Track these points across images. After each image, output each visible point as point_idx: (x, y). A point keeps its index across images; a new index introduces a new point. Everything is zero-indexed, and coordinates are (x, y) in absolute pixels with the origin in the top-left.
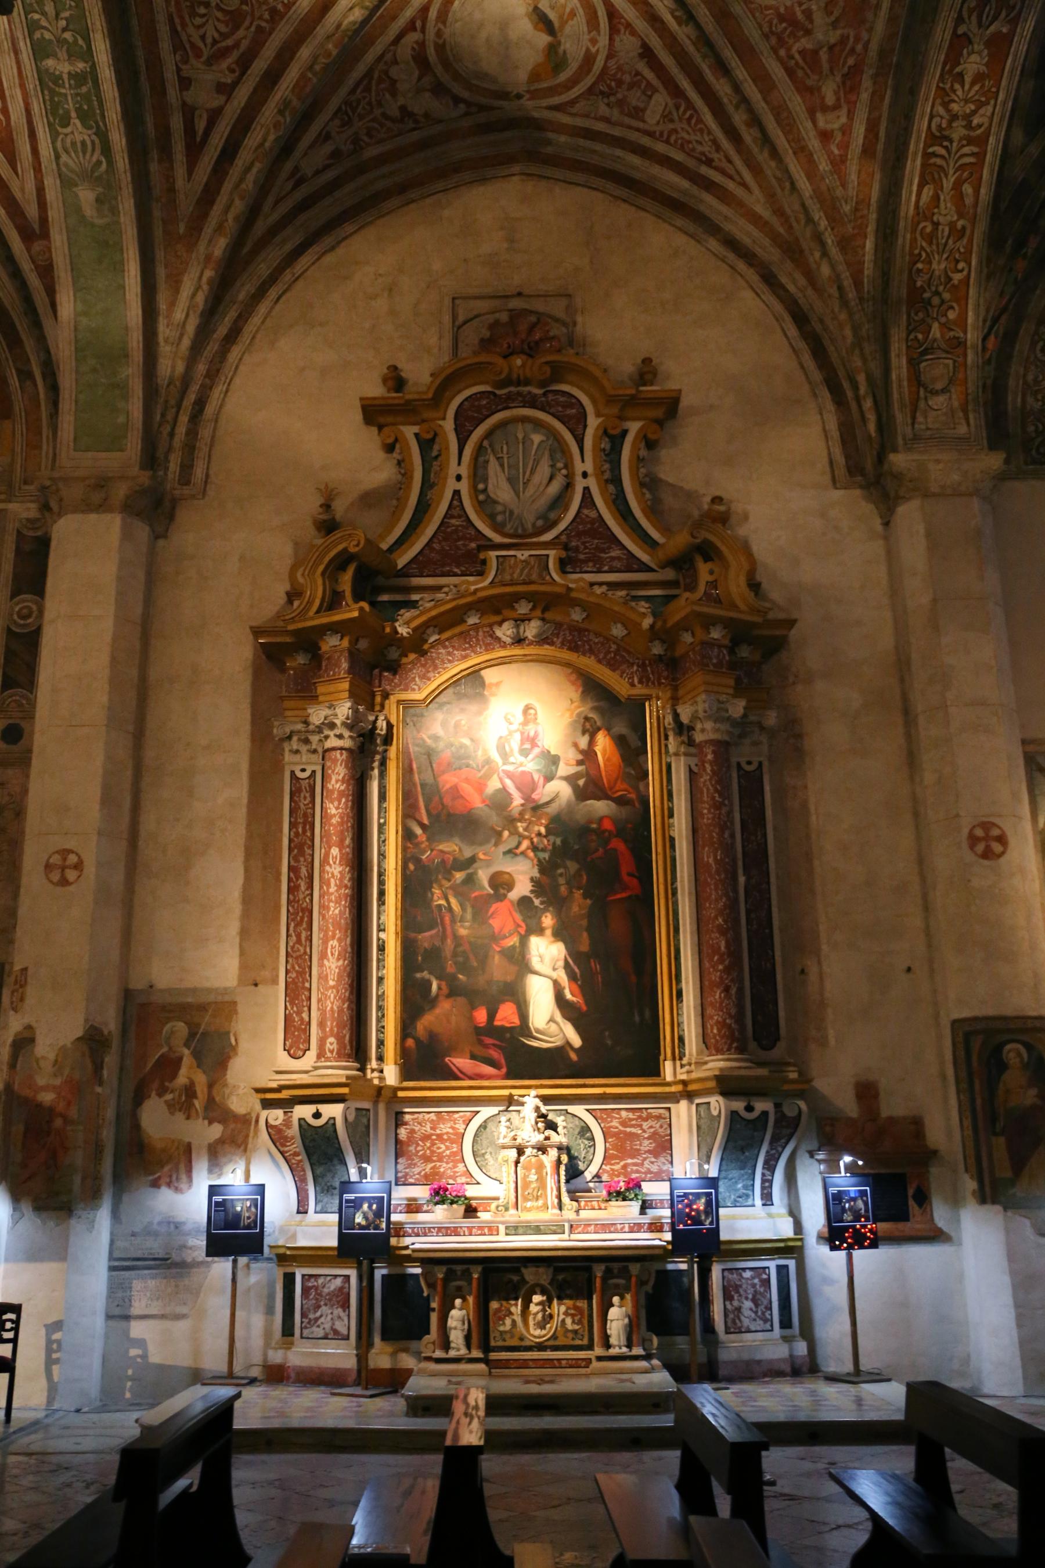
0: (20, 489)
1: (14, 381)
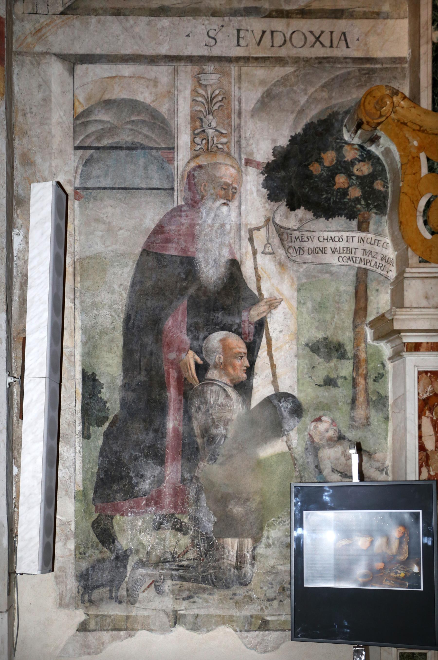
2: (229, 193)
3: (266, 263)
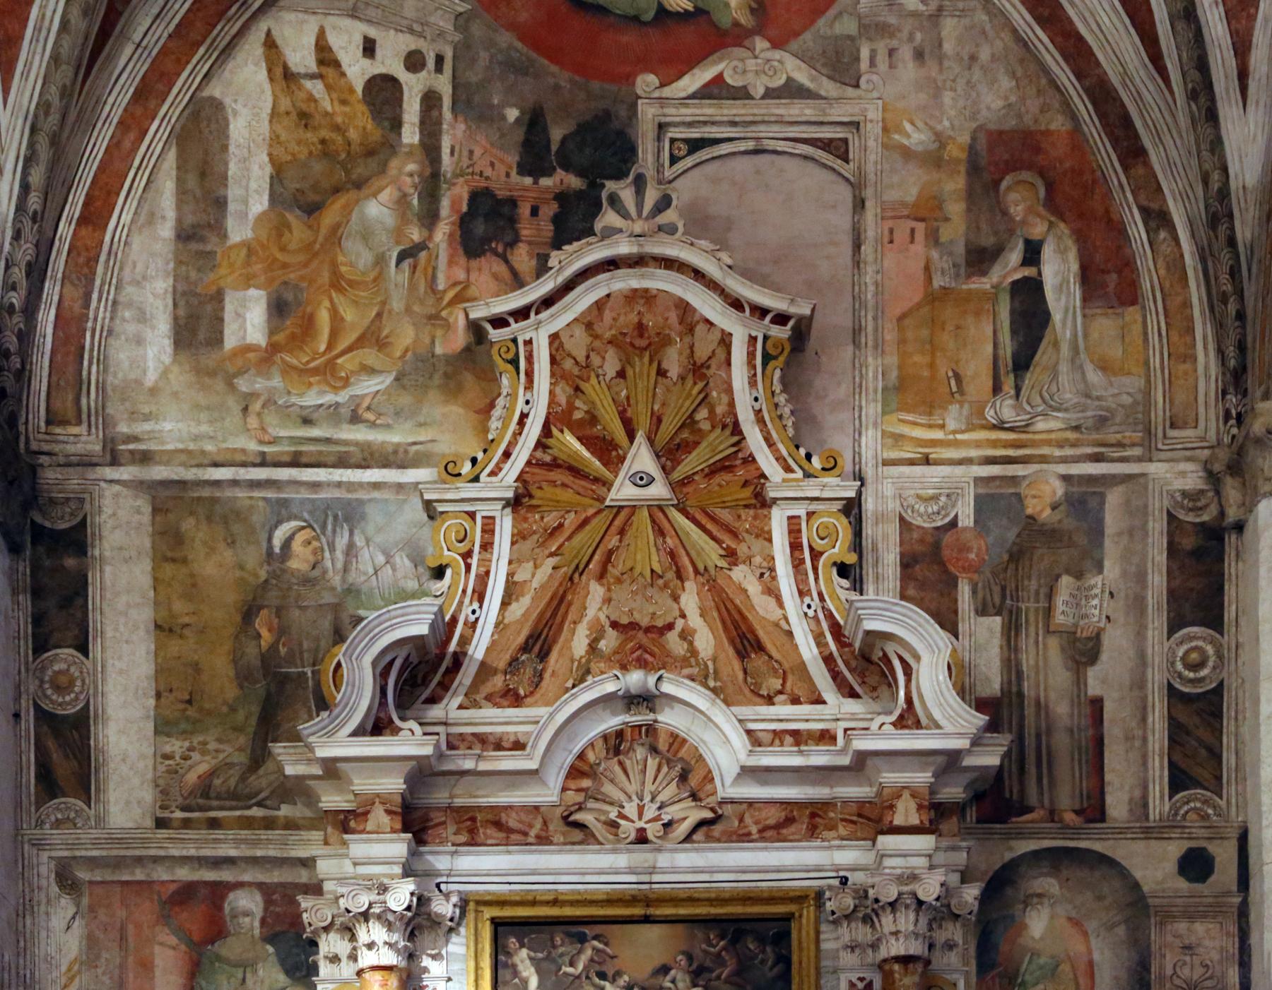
0: (1165, 436)
1: (1137, 230)
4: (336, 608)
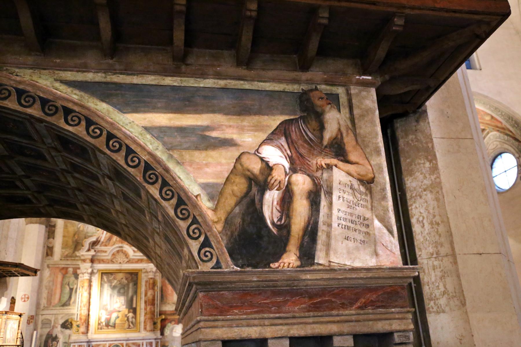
2: (57, 327)
3: (60, 334)
4: (85, 234)
